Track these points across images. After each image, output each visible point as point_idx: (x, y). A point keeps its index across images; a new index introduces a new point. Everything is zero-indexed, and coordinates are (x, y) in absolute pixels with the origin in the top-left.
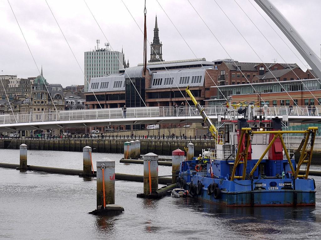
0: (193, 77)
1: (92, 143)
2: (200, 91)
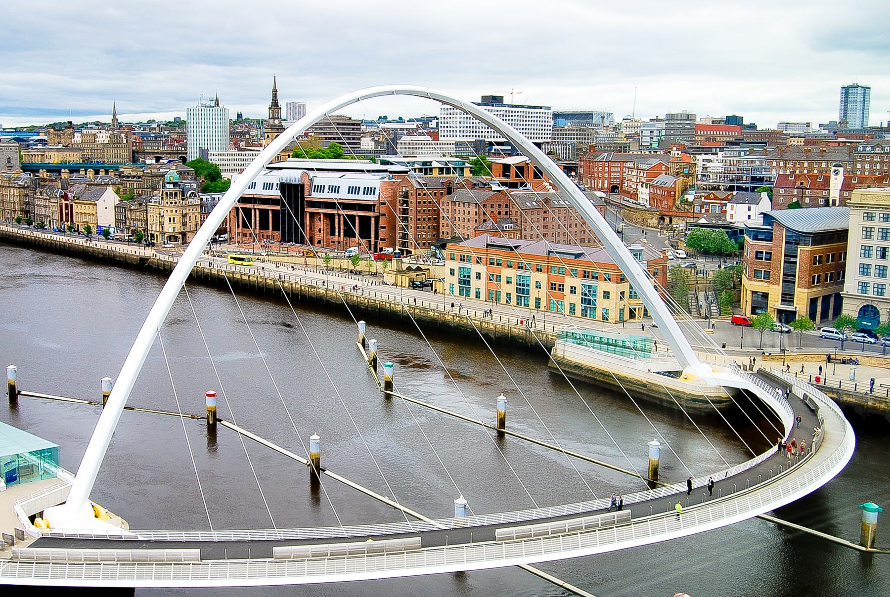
0: (365, 188)
1: (266, 281)
2: (374, 205)
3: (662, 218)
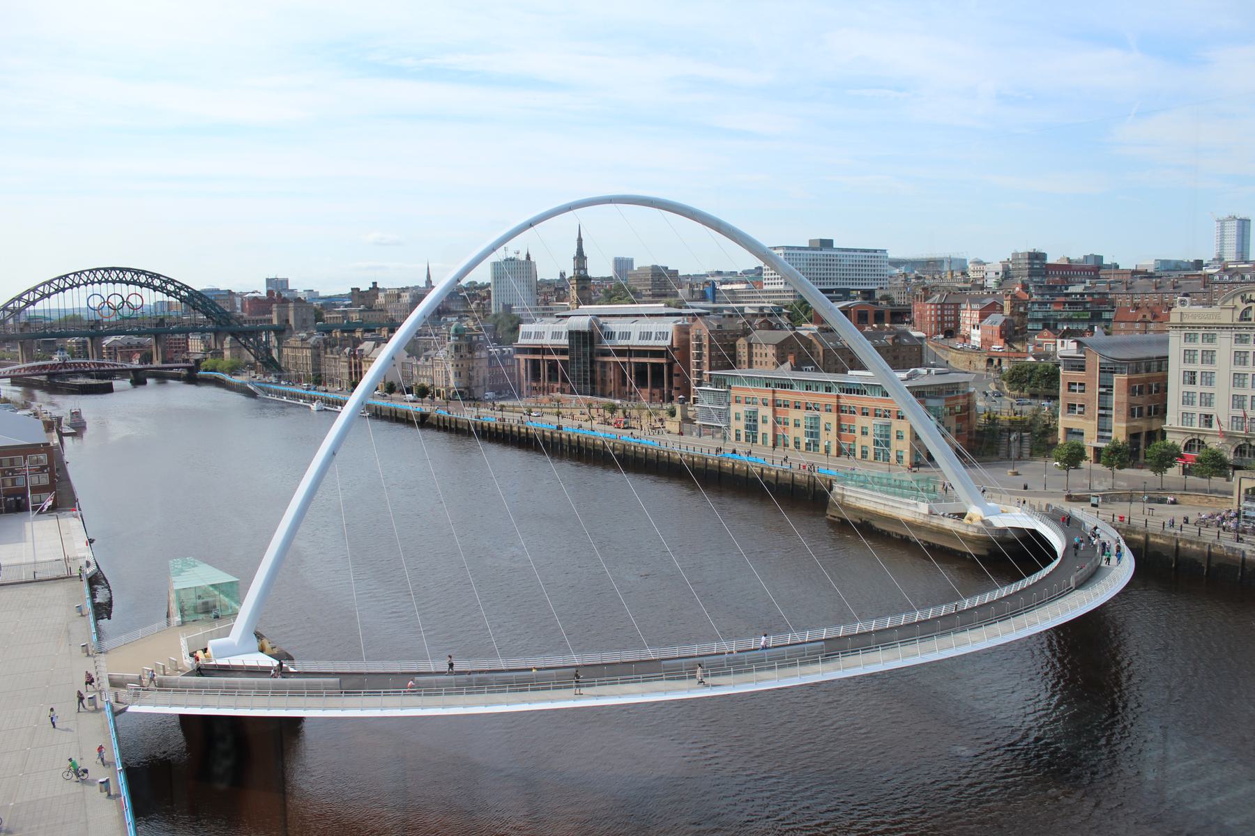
3: (990, 361)
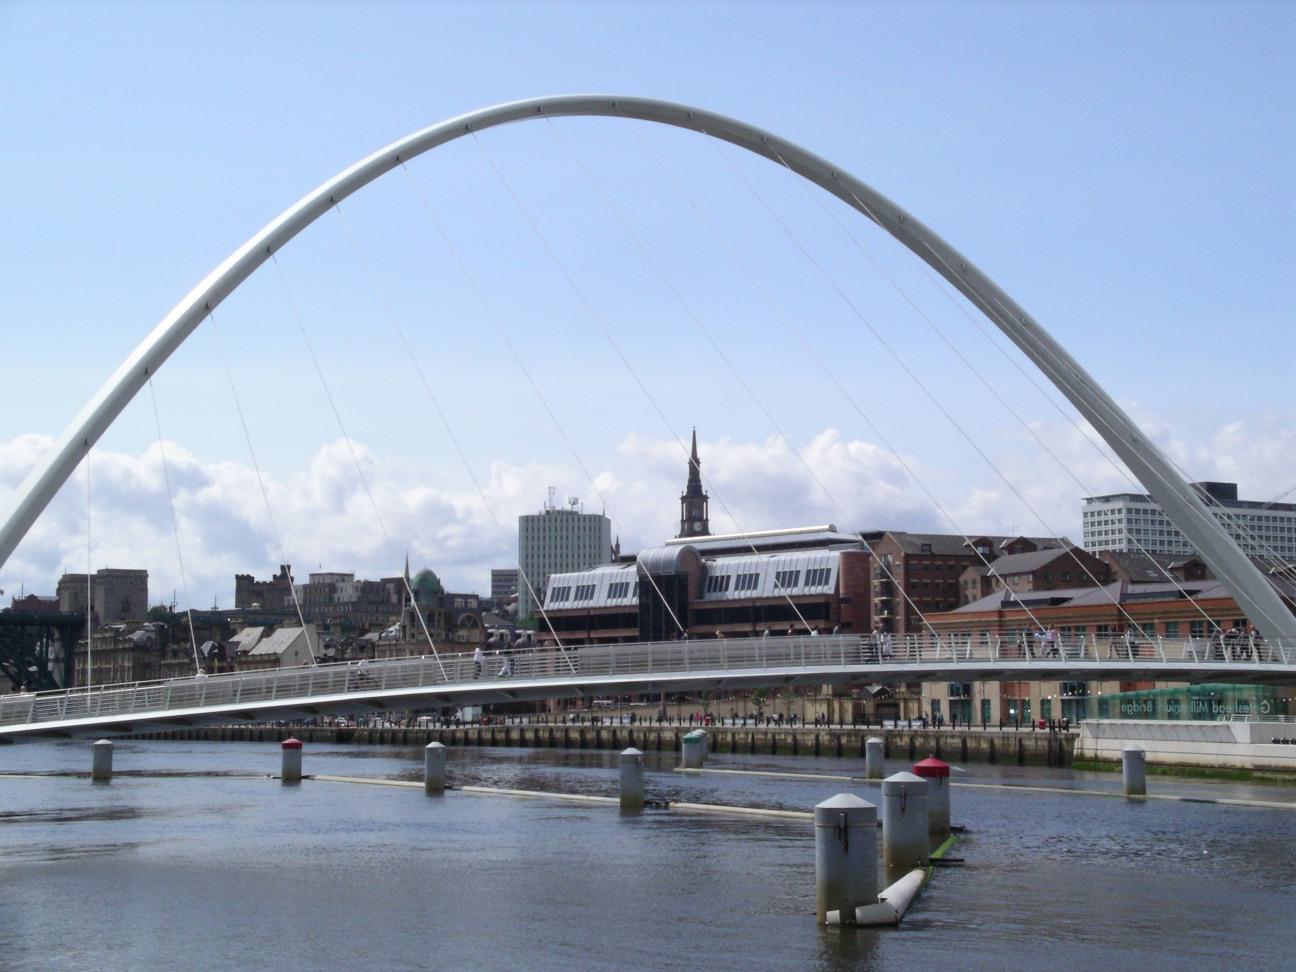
2: (827, 605)
